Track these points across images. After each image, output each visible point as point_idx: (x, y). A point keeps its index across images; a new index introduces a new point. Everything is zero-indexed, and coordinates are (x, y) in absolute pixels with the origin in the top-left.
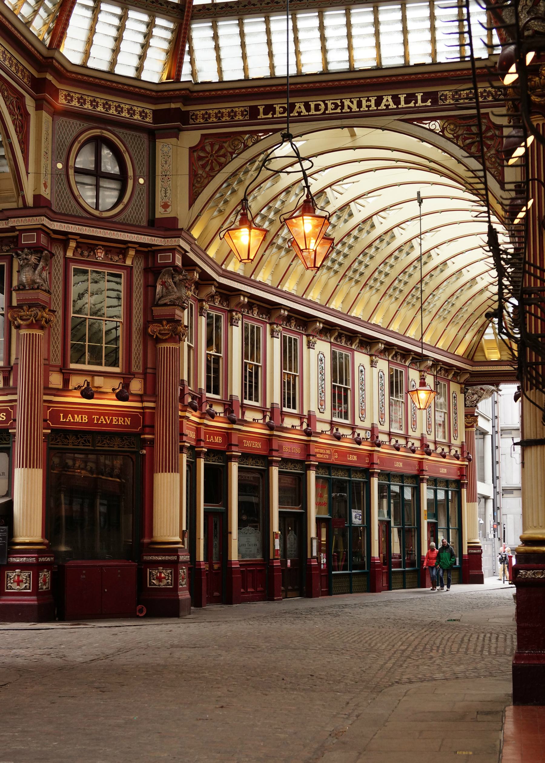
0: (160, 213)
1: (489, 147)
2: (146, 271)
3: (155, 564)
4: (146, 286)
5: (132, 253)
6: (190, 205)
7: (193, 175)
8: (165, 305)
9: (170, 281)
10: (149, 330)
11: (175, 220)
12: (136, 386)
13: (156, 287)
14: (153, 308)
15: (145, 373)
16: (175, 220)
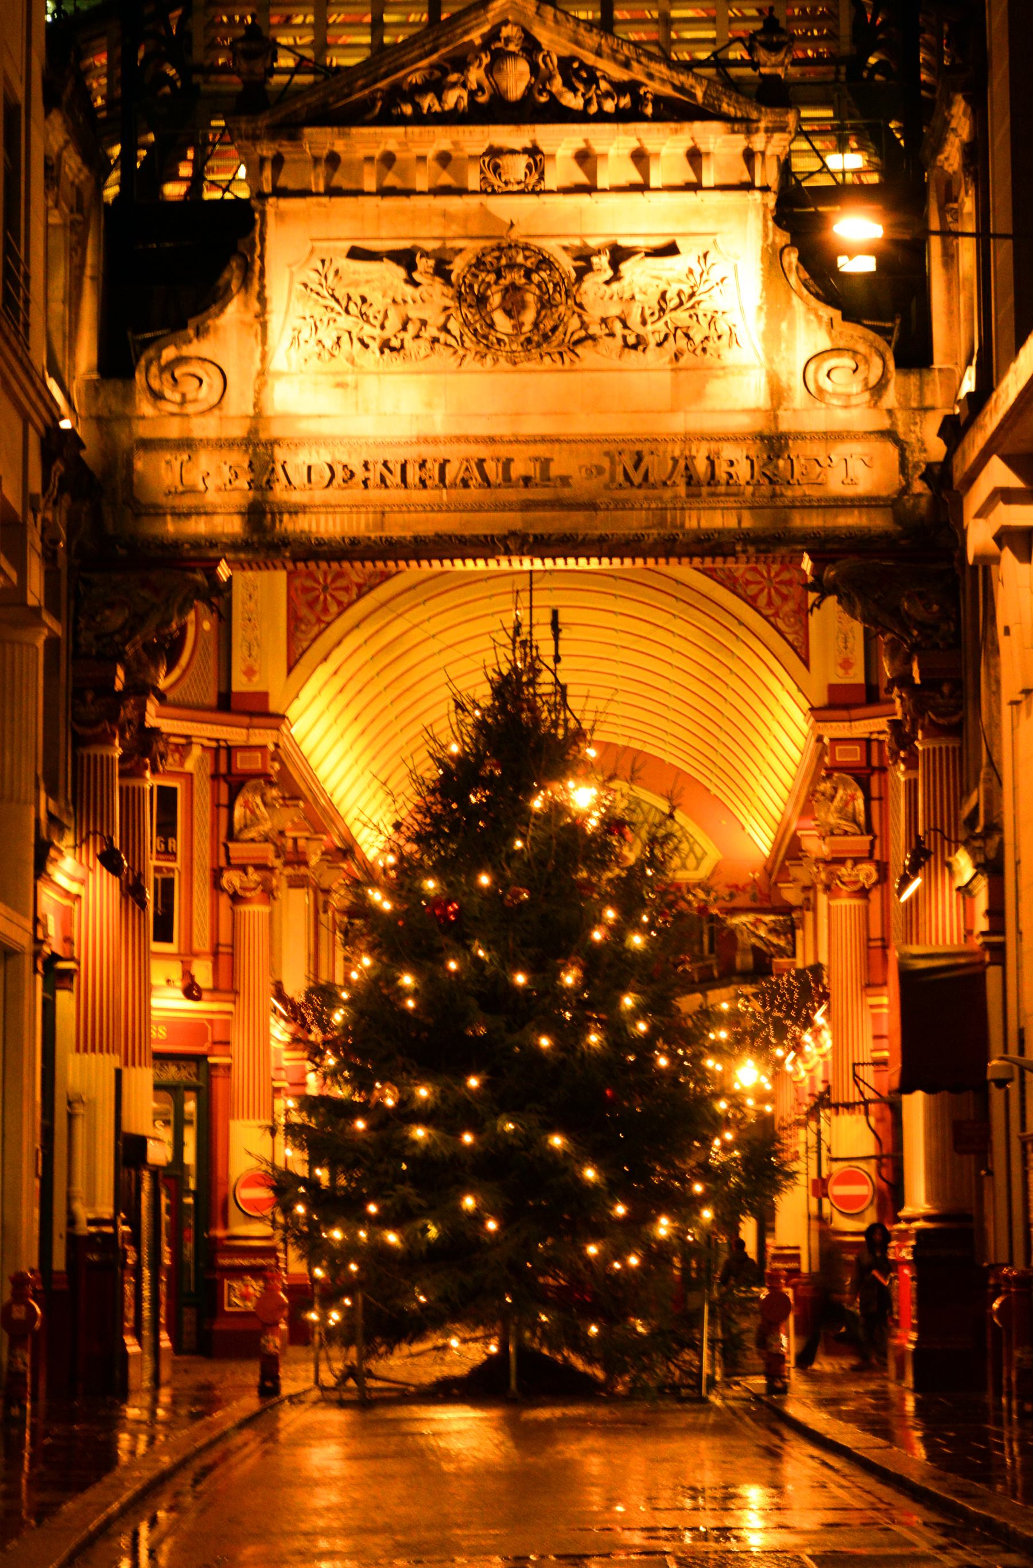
0: (240, 684)
1: (785, 598)
2: (215, 777)
3: (238, 1272)
4: (216, 805)
5: (196, 751)
6: (290, 670)
7: (294, 620)
8: (253, 840)
9: (258, 800)
10: (224, 882)
11: (264, 696)
12: (203, 974)
13: (231, 808)
14: (231, 845)
15: (215, 954)
16: (264, 696)
